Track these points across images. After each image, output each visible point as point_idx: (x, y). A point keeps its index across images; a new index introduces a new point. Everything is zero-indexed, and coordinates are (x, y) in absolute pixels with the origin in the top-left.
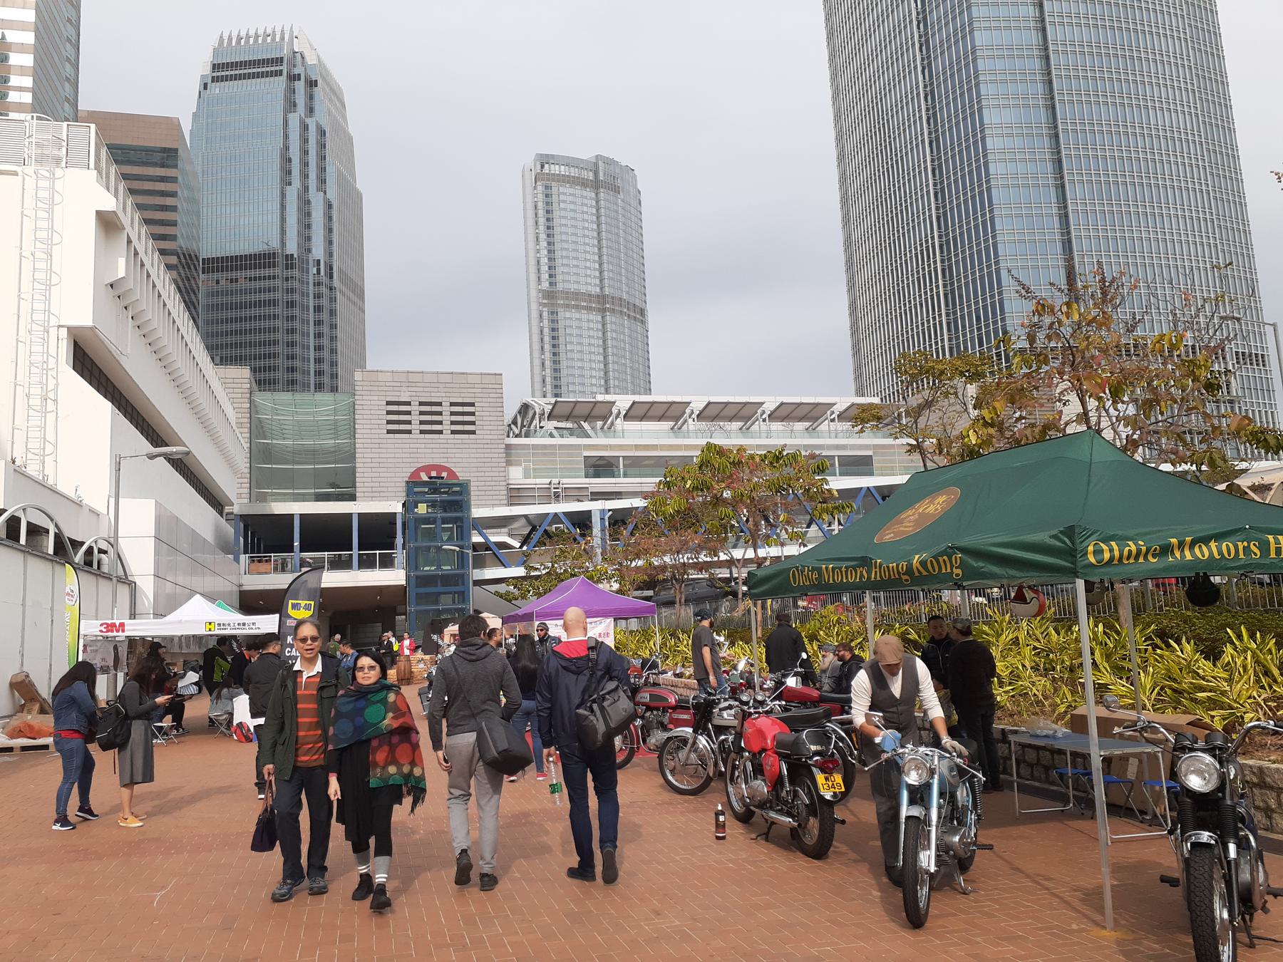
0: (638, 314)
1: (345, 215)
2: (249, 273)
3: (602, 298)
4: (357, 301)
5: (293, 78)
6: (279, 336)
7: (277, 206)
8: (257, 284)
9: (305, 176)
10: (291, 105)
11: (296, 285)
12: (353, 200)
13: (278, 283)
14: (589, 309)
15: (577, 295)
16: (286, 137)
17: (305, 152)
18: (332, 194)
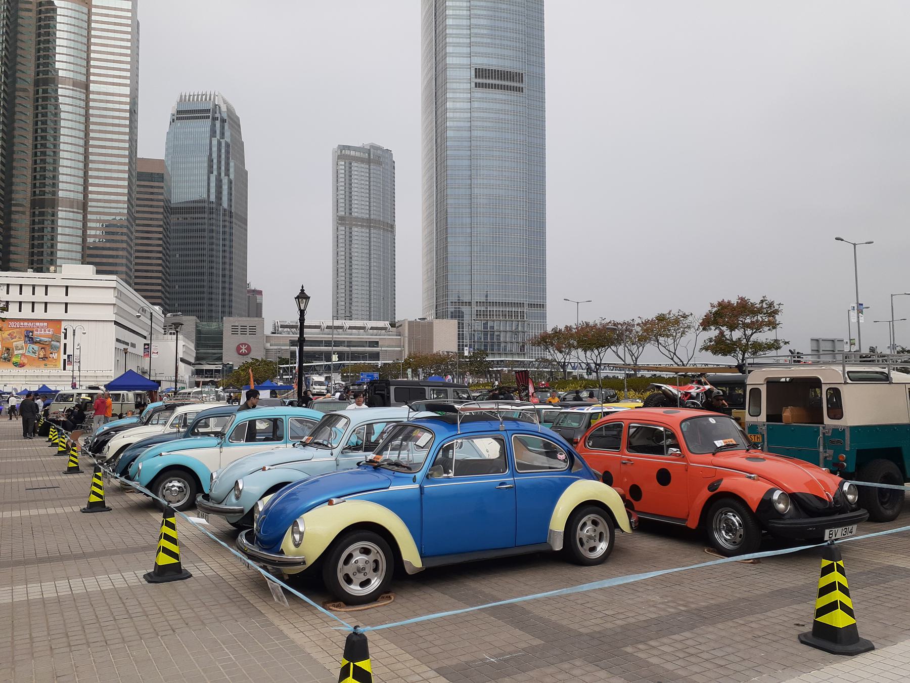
0: (390, 228)
1: (240, 184)
2: (192, 215)
3: (369, 220)
4: (243, 226)
5: (215, 119)
6: (205, 308)
7: (206, 184)
8: (197, 221)
9: (219, 168)
10: (213, 133)
11: (214, 222)
12: (243, 175)
13: (206, 221)
14: (362, 226)
15: (356, 218)
16: (211, 149)
17: (219, 156)
18: (232, 176)
